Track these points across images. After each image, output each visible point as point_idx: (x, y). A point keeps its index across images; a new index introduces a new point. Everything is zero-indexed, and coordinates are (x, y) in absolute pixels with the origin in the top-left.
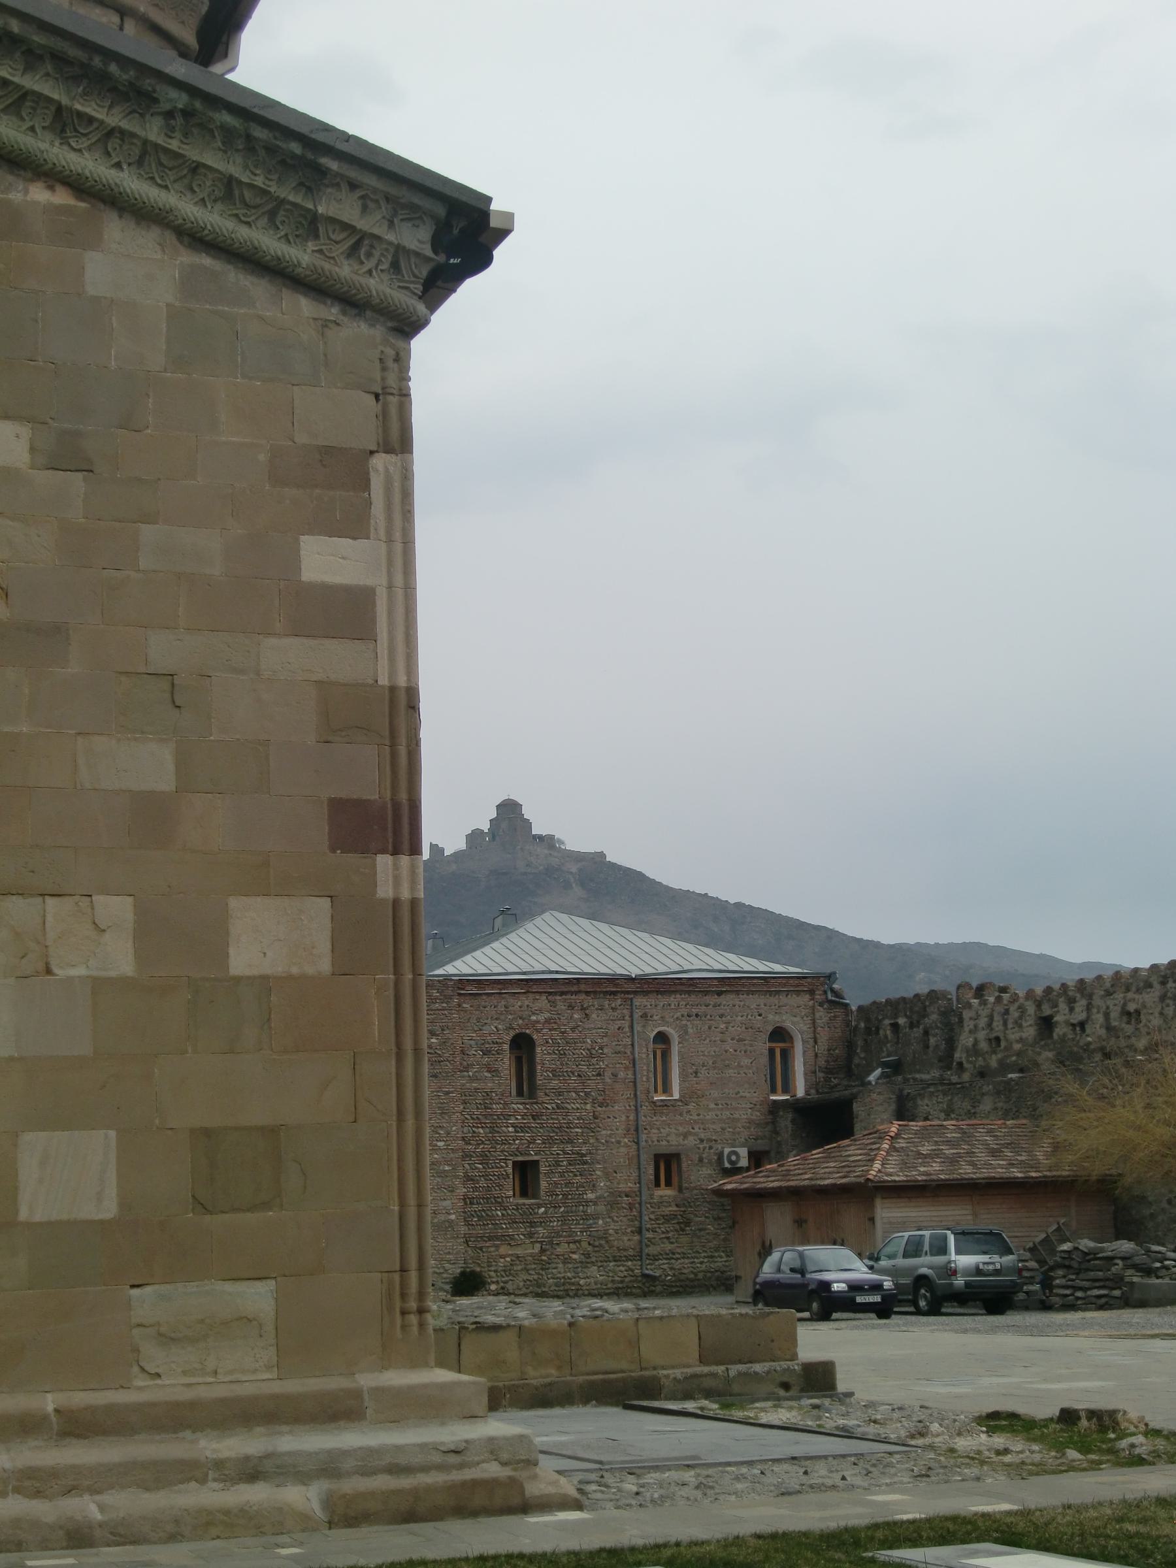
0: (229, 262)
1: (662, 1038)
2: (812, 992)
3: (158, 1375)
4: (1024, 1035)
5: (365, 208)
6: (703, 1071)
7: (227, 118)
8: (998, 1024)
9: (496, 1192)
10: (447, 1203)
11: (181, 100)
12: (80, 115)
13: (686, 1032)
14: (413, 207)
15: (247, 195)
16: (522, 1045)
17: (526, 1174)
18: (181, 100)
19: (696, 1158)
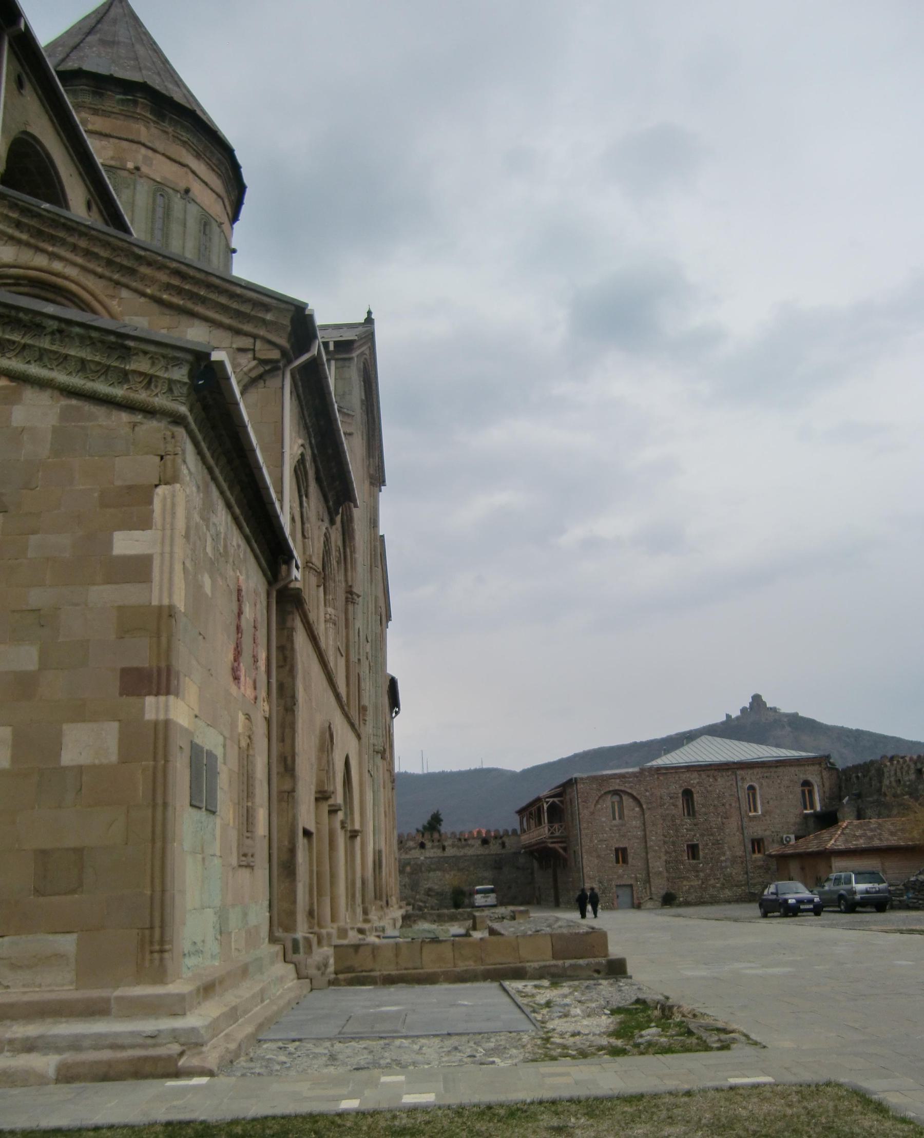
0: (85, 401)
1: (751, 788)
2: (820, 764)
3: (8, 987)
4: (911, 778)
5: (153, 364)
6: (771, 802)
7: (77, 330)
8: (899, 773)
9: (680, 858)
10: (658, 863)
11: (54, 325)
12: (9, 341)
13: (762, 784)
14: (177, 359)
15: (93, 367)
16: (688, 794)
17: (693, 850)
18: (54, 325)
19: (771, 840)
